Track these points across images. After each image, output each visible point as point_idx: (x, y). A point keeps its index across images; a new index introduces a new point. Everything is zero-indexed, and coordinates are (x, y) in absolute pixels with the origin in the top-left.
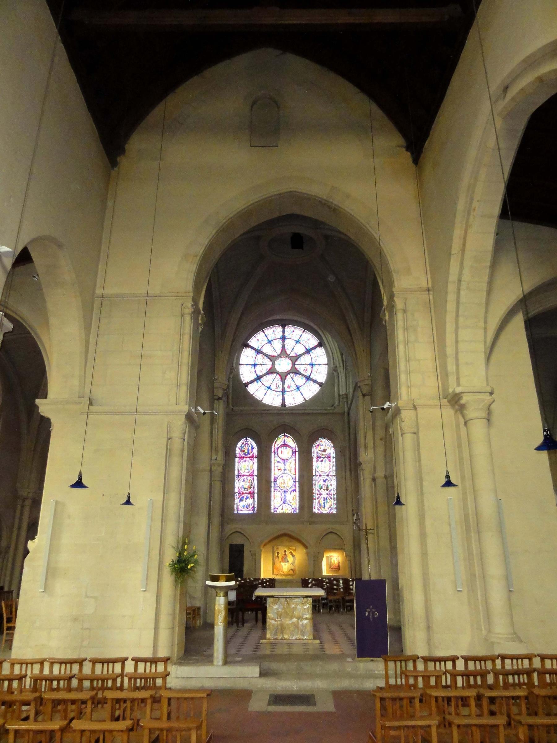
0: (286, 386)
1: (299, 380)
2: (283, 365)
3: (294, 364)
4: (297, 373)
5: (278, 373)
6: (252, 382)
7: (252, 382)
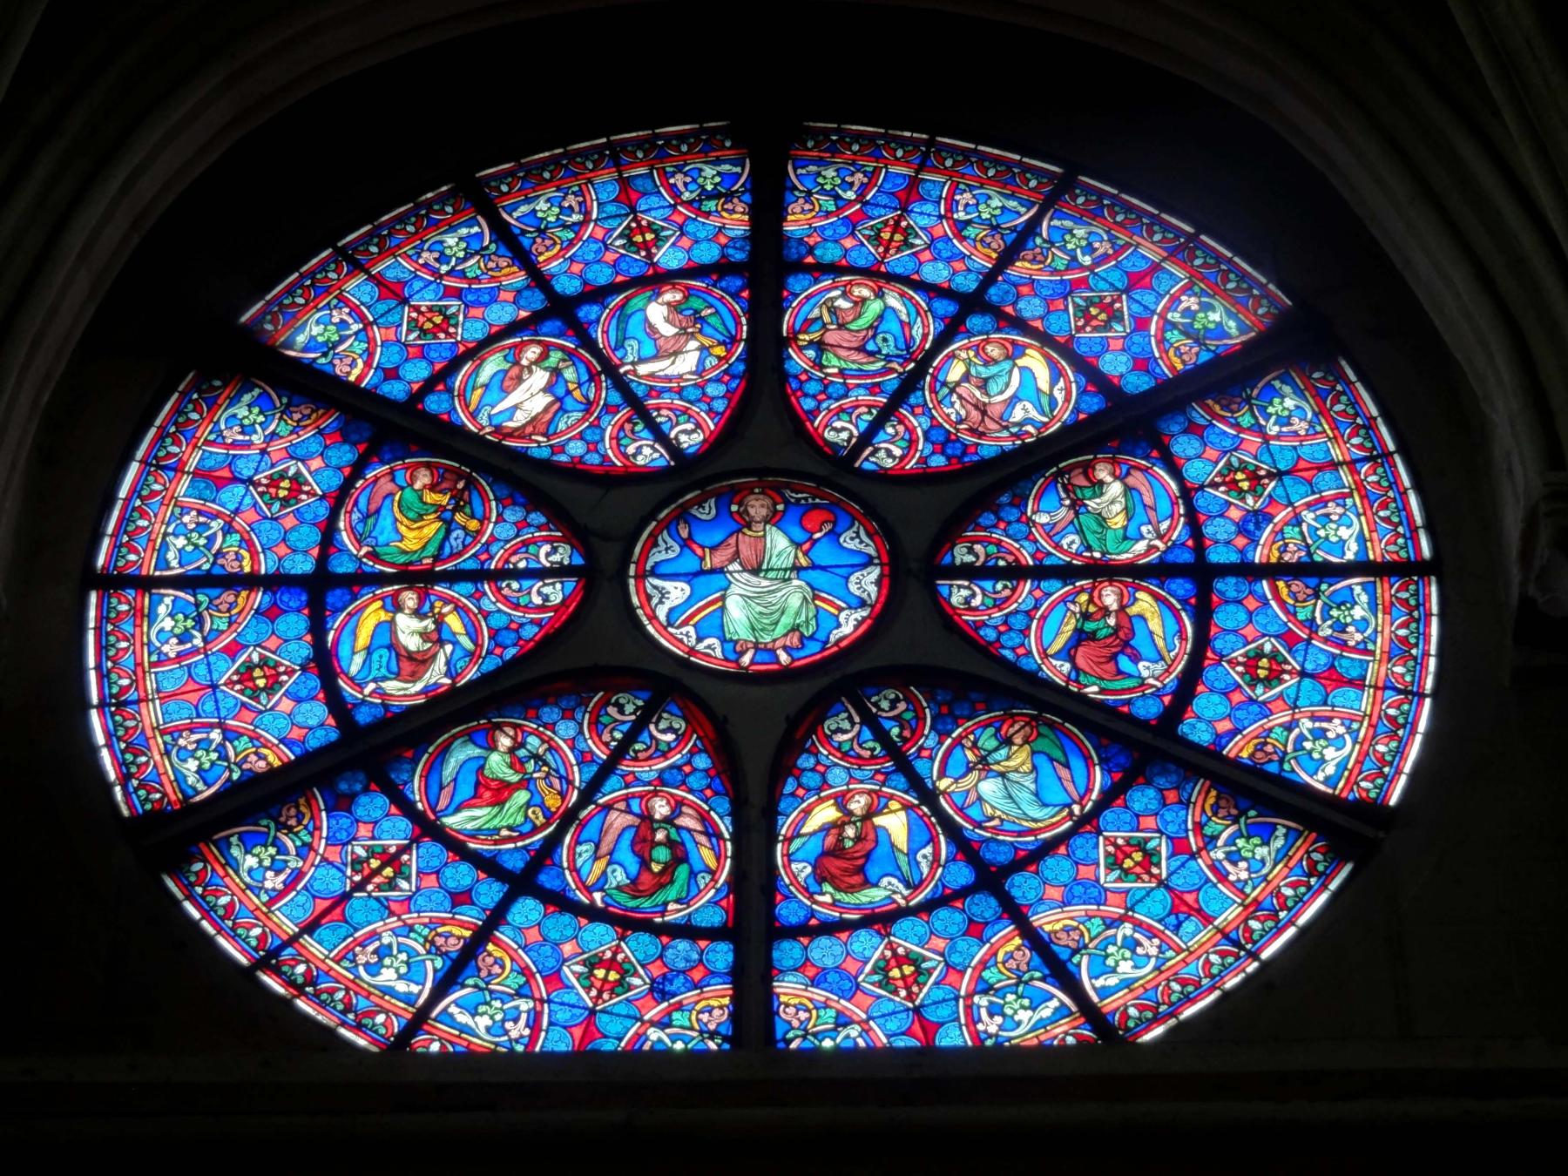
0: (796, 866)
1: (1011, 787)
2: (760, 596)
3: (913, 572)
4: (989, 687)
5: (669, 683)
6: (257, 802)
7: (257, 802)
